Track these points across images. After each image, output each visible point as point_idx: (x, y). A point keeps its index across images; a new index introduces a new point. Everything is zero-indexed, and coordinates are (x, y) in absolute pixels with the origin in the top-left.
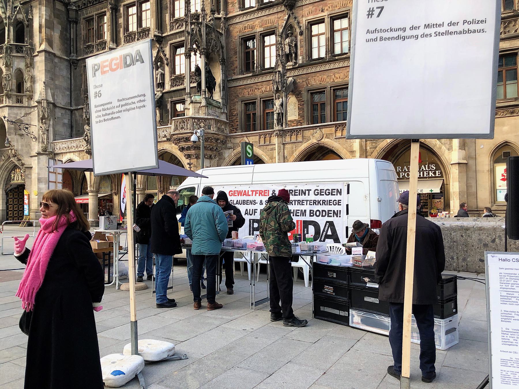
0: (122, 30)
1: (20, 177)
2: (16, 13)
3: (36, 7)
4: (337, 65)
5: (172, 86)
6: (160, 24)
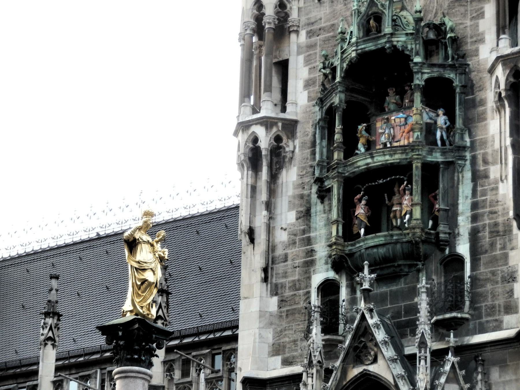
2: (443, 380)
3: (503, 365)
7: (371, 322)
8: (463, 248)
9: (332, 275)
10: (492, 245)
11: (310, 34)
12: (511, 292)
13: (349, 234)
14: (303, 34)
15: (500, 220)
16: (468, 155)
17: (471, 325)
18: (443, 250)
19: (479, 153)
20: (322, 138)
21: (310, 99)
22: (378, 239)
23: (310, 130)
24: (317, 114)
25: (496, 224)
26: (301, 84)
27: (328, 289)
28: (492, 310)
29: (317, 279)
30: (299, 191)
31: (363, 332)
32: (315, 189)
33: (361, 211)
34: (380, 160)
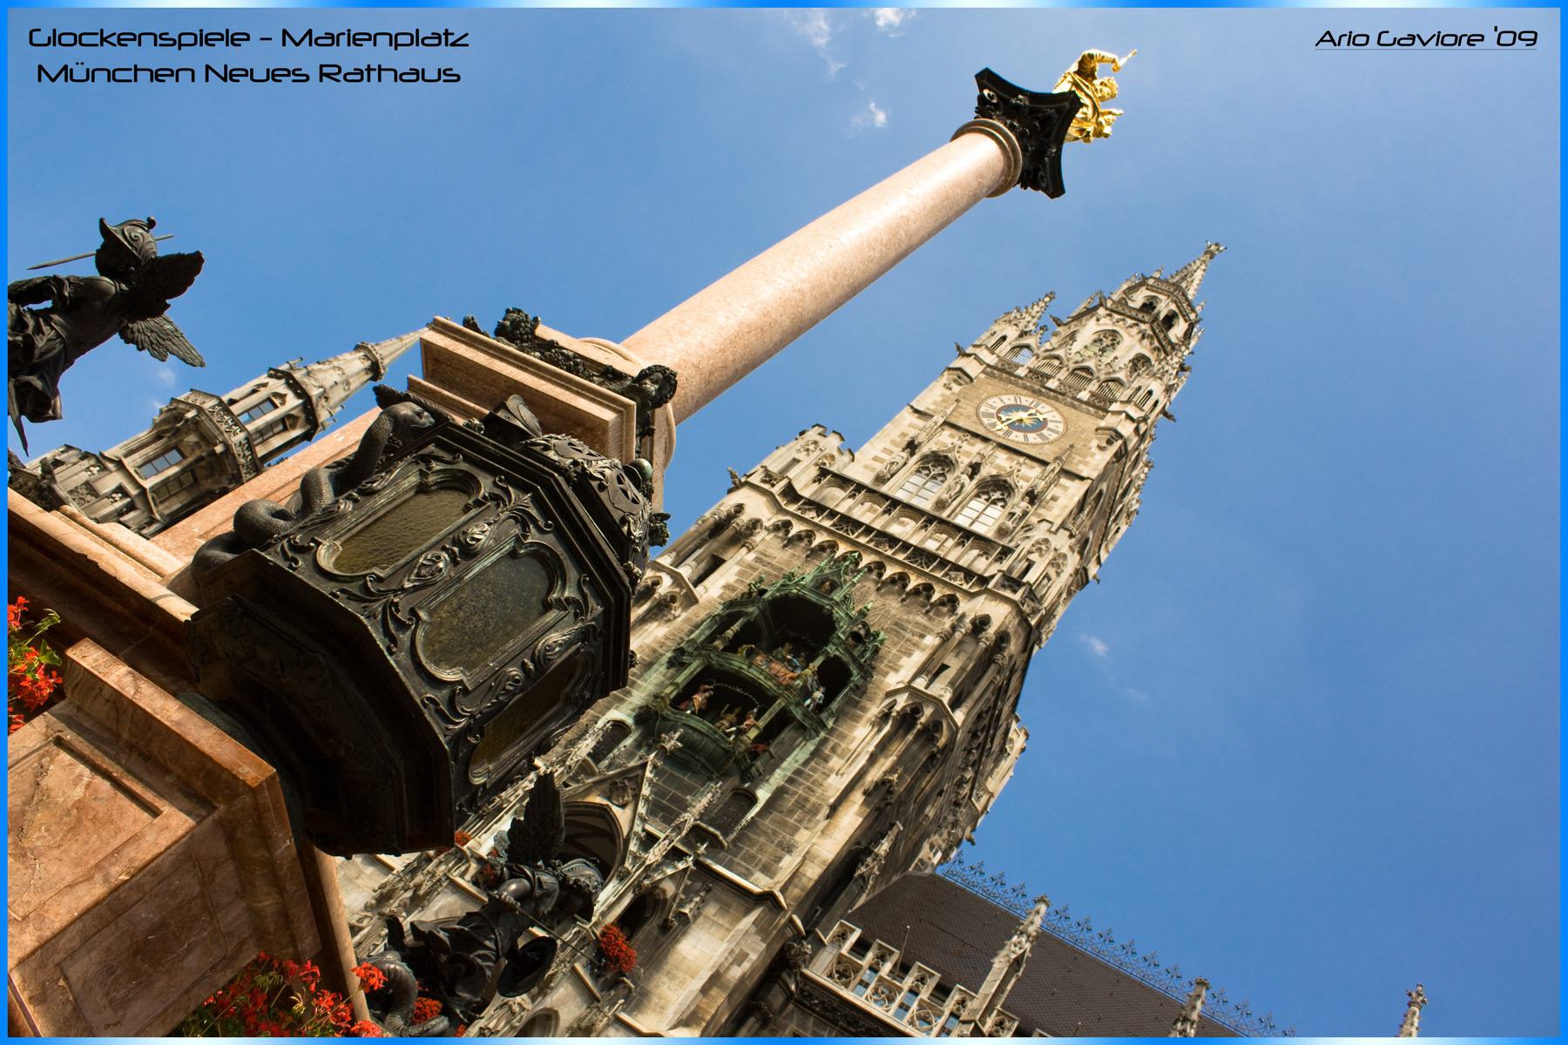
3: (725, 908)
7: (648, 774)
8: (763, 794)
9: (630, 721)
10: (791, 812)
11: (757, 560)
12: (780, 859)
14: (752, 556)
15: (813, 799)
16: (822, 734)
17: (722, 854)
18: (743, 781)
19: (833, 740)
20: (709, 627)
21: (721, 596)
22: (703, 725)
23: (702, 615)
24: (719, 609)
25: (806, 800)
26: (722, 582)
27: (619, 729)
28: (751, 859)
30: (656, 646)
31: (633, 778)
32: (669, 654)
33: (699, 699)
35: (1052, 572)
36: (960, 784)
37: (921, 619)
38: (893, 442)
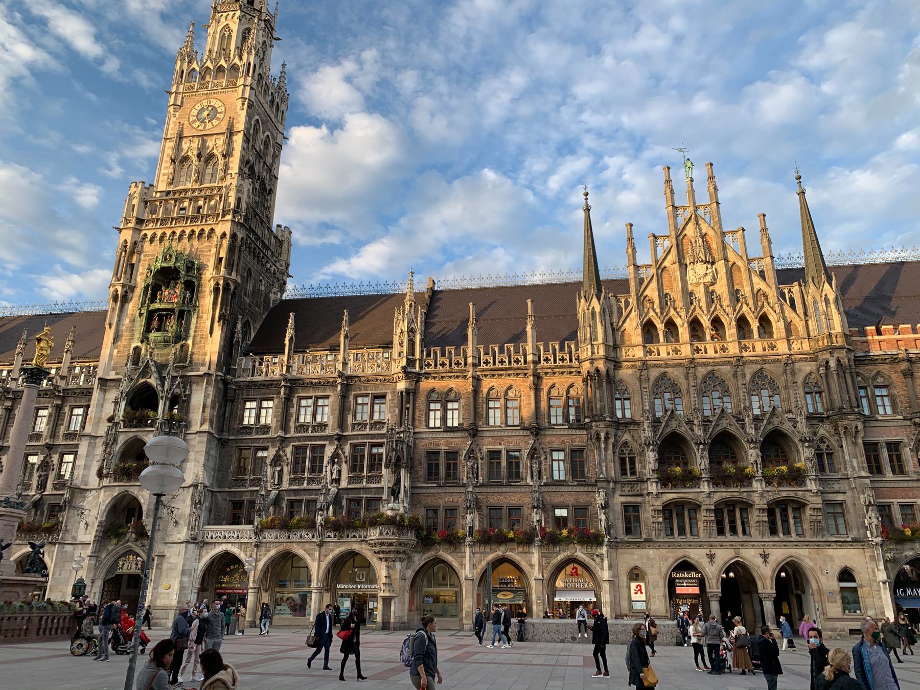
0: (293, 420)
1: (134, 566)
3: (197, 383)
4: (512, 489)
5: (349, 483)
6: (342, 424)
9: (139, 344)
13: (148, 330)
27: (137, 349)
29: (133, 345)
31: (147, 366)
34: (163, 306)
35: (240, 195)
36: (268, 270)
37: (207, 244)
38: (166, 162)
